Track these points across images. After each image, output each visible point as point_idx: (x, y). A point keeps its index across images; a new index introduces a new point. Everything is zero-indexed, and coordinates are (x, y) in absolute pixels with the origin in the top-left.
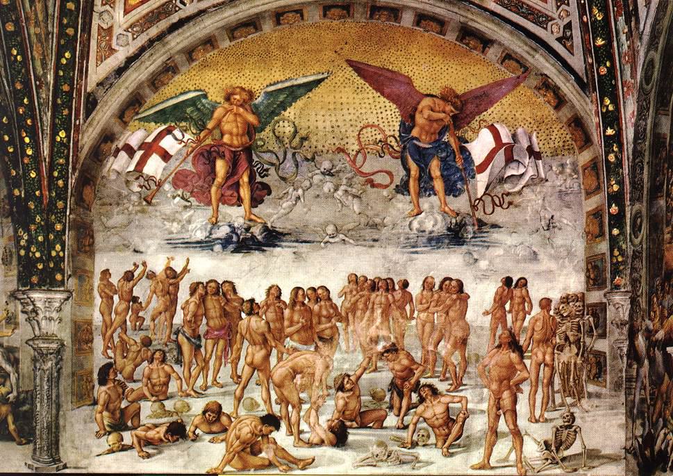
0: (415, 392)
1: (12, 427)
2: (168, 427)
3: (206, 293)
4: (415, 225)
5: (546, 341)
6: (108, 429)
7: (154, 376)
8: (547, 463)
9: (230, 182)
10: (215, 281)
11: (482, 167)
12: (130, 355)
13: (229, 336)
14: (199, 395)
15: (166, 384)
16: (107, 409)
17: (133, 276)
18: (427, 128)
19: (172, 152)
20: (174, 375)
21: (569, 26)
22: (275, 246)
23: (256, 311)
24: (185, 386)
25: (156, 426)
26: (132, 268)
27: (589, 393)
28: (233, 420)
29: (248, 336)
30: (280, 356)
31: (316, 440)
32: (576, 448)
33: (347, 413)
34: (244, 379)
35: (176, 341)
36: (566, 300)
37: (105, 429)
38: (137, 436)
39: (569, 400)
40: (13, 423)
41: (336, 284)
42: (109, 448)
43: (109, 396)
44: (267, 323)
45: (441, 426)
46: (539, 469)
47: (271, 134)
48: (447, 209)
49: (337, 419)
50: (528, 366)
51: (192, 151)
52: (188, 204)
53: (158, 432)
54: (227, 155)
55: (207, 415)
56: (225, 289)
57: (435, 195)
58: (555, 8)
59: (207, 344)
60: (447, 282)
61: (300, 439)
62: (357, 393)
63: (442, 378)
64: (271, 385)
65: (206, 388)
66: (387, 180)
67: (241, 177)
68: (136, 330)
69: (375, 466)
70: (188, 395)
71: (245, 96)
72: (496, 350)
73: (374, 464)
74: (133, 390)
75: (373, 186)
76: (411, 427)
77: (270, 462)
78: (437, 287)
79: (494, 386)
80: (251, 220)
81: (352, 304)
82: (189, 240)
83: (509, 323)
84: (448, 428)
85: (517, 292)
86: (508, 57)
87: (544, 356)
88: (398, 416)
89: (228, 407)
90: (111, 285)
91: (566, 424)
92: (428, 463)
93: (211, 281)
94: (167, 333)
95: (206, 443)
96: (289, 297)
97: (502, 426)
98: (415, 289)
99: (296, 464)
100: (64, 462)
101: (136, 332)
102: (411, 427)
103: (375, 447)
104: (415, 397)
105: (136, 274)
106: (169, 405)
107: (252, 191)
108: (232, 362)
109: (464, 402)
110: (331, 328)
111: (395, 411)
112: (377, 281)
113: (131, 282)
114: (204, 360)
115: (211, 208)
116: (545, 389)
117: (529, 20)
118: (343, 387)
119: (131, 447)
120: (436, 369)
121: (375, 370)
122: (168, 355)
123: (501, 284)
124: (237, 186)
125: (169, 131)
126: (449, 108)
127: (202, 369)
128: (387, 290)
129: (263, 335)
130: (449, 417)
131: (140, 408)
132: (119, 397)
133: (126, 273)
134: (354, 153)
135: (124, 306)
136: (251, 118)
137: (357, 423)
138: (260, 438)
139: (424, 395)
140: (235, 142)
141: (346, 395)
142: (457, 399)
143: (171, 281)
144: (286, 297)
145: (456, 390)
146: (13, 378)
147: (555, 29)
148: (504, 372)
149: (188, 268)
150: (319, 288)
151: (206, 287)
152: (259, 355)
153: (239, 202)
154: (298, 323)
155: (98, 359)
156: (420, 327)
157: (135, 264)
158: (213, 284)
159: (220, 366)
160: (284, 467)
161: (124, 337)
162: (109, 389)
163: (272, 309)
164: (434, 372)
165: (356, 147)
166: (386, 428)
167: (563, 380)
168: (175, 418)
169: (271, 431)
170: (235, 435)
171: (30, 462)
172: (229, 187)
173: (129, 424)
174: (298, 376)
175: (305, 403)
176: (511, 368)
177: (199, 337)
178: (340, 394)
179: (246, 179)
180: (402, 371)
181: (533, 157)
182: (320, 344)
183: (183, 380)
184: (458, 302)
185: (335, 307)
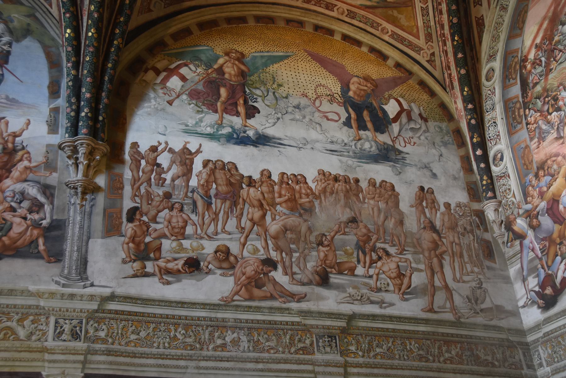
0: (374, 252)
1: (42, 247)
2: (186, 261)
3: (215, 168)
4: (359, 146)
5: (453, 228)
6: (133, 257)
7: (174, 220)
8: (472, 313)
9: (230, 102)
10: (222, 161)
11: (395, 119)
12: (154, 203)
13: (233, 198)
14: (210, 238)
15: (184, 228)
16: (133, 241)
17: (157, 149)
18: (358, 93)
19: (188, 77)
20: (190, 221)
21: (433, 54)
22: (264, 145)
23: (254, 184)
24: (199, 231)
25: (175, 259)
26: (156, 144)
27: (487, 266)
28: (239, 260)
29: (248, 200)
30: (273, 216)
31: (306, 280)
32: (487, 304)
33: (327, 262)
34: (246, 231)
35: (192, 198)
36: (459, 205)
37: (130, 257)
38: (158, 266)
39: (476, 269)
40: (44, 244)
41: (311, 175)
42: (133, 273)
43: (135, 231)
44: (262, 193)
45: (395, 278)
46: (467, 316)
47: (258, 79)
48: (377, 140)
49: (321, 266)
50: (445, 243)
51: (202, 80)
52: (200, 110)
53: (177, 265)
54: (228, 85)
55: (218, 254)
56: (230, 167)
57: (369, 130)
59: (216, 204)
60: (384, 183)
61: (293, 279)
62: (333, 249)
63: (390, 244)
64: (268, 237)
65: (217, 234)
66: (336, 118)
67: (238, 100)
68: (158, 186)
69: (353, 303)
70: (202, 238)
71: (238, 55)
72: (422, 230)
73: (352, 302)
74: (156, 230)
75: (328, 119)
76: (375, 277)
77: (271, 294)
78: (378, 185)
79: (427, 254)
80: (246, 126)
81: (322, 188)
82: (202, 132)
83: (428, 215)
84: (400, 279)
85: (428, 196)
86: (398, 65)
87: (454, 237)
88: (365, 267)
89: (235, 248)
90: (139, 153)
91: (478, 286)
92: (391, 305)
93: (218, 160)
94: (185, 190)
95: (217, 276)
96: (278, 177)
97: (437, 283)
98: (364, 185)
99: (292, 298)
100: (92, 281)
101: (159, 187)
102: (375, 277)
103: (351, 289)
104: (374, 256)
105: (160, 149)
106: (186, 243)
107: (246, 110)
108: (237, 217)
109: (408, 262)
110: (309, 202)
111: (362, 263)
112: (338, 176)
113: (156, 153)
114: (215, 213)
115: (217, 114)
116: (459, 260)
118: (322, 243)
119: (153, 275)
120: (386, 238)
121: (345, 234)
122: (185, 206)
123: (418, 190)
124: (236, 104)
125: (186, 65)
126: (369, 85)
127: (213, 220)
128: (346, 182)
129: (259, 201)
130: (400, 272)
131: (161, 244)
132: (144, 233)
133: (152, 147)
134: (314, 99)
135: (149, 168)
136: (243, 67)
137: (335, 269)
138: (262, 275)
139: (380, 255)
140: (233, 79)
141: (325, 249)
142: (403, 260)
143: (187, 157)
144: (275, 177)
145: (401, 253)
146: (47, 208)
147: (425, 55)
148: (431, 245)
149: (201, 150)
150: (298, 175)
151: (215, 164)
152: (257, 214)
153: (238, 114)
154: (285, 196)
155: (128, 204)
156: (370, 209)
157: (159, 142)
158: (220, 163)
159: (228, 218)
160: (283, 299)
161: (149, 189)
162: (135, 226)
163: (265, 184)
164: (385, 240)
165: (315, 96)
166: (357, 276)
167: (469, 255)
168: (191, 254)
169: (270, 271)
170: (242, 271)
171: (57, 279)
172: (230, 105)
173: (152, 255)
174: (288, 232)
175: (296, 252)
176: (436, 245)
177: (210, 197)
178: (320, 247)
179: (241, 101)
180: (363, 236)
181: (423, 121)
182: (302, 211)
183: (198, 226)
184: (393, 197)
185: (311, 189)
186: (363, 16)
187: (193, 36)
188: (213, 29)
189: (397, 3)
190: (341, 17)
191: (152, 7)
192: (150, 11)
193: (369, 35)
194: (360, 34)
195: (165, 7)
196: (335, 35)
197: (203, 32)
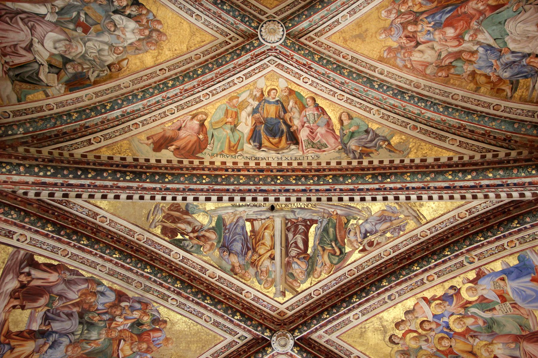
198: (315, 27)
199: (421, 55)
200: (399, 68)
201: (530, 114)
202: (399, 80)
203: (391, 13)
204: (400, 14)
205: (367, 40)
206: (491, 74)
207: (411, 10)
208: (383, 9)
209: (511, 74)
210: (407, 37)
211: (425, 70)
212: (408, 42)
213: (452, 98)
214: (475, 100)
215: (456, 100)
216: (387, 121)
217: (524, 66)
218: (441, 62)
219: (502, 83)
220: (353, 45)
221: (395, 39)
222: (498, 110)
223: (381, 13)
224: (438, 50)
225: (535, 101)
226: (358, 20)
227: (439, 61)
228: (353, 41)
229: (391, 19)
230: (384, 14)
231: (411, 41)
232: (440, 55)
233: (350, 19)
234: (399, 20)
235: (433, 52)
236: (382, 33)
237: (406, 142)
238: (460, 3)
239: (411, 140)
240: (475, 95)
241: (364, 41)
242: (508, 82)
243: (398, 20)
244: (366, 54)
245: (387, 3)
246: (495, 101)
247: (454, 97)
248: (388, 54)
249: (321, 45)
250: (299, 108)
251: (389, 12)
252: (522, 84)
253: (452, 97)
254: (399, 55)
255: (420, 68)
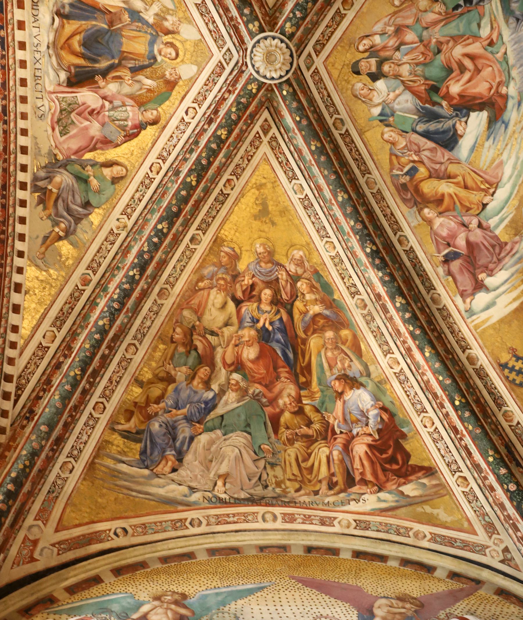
58: (487, 539)
117: (466, 550)
186: (381, 523)
187: (103, 584)
188: (138, 572)
189: (426, 496)
190: (346, 531)
191: (36, 555)
192: (33, 560)
193: (397, 545)
194: (382, 546)
195: (59, 554)
196: (341, 553)
197: (120, 578)
198: (286, 136)
199: (218, 306)
200: (199, 268)
201: (75, 452)
202: (178, 267)
203: (297, 265)
204: (294, 279)
205: (256, 224)
206: (162, 405)
207: (297, 296)
208: (307, 253)
209: (154, 432)
210: (253, 287)
211: (191, 308)
212: (244, 288)
213: (129, 345)
214: (121, 378)
215: (126, 350)
216: (103, 238)
217: (164, 452)
218: (199, 335)
219: (141, 418)
220: (250, 198)
221: (252, 267)
222: (94, 409)
223: (299, 249)
224: (222, 332)
225: (96, 461)
226: (293, 212)
227: (202, 332)
228: (257, 199)
229: (287, 265)
230: (298, 254)
231: (244, 292)
232: (213, 333)
233: (295, 198)
234: (284, 277)
235: (220, 324)
236: (265, 248)
237: (61, 264)
238: (295, 371)
239: (64, 274)
240: (129, 378)
241: (256, 217)
242: (142, 427)
243: (283, 276)
244: (231, 218)
245: (315, 260)
246: (111, 407)
247: (133, 347)
248: (226, 253)
249: (255, 144)
250: (140, 95)
251: (300, 263)
252: (133, 446)
253: (134, 345)
254: (222, 270)
255: (195, 302)
